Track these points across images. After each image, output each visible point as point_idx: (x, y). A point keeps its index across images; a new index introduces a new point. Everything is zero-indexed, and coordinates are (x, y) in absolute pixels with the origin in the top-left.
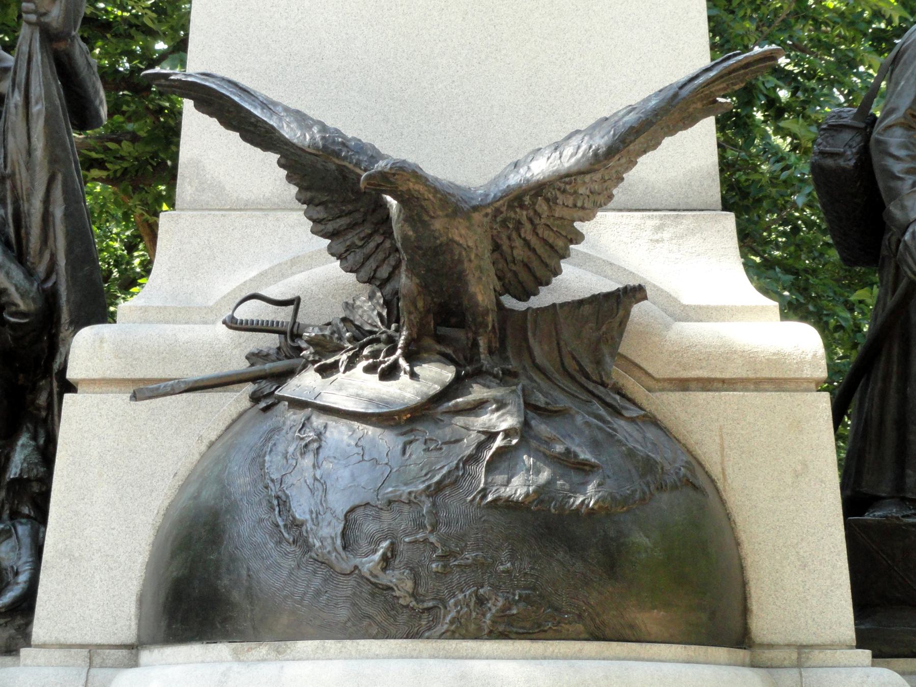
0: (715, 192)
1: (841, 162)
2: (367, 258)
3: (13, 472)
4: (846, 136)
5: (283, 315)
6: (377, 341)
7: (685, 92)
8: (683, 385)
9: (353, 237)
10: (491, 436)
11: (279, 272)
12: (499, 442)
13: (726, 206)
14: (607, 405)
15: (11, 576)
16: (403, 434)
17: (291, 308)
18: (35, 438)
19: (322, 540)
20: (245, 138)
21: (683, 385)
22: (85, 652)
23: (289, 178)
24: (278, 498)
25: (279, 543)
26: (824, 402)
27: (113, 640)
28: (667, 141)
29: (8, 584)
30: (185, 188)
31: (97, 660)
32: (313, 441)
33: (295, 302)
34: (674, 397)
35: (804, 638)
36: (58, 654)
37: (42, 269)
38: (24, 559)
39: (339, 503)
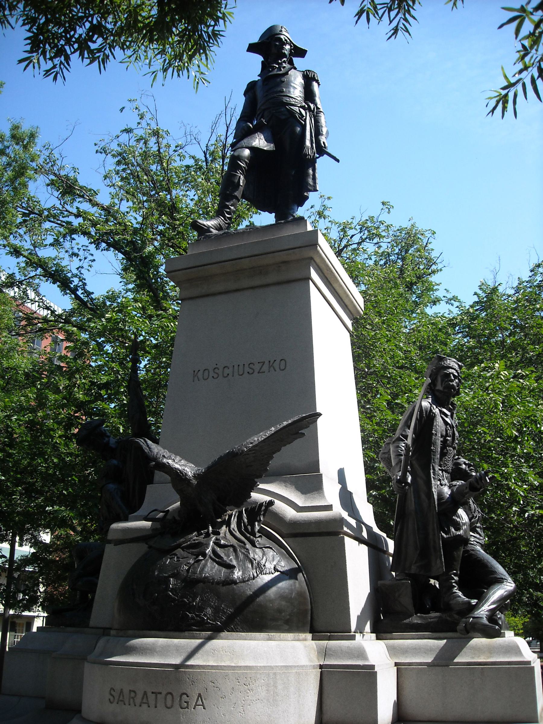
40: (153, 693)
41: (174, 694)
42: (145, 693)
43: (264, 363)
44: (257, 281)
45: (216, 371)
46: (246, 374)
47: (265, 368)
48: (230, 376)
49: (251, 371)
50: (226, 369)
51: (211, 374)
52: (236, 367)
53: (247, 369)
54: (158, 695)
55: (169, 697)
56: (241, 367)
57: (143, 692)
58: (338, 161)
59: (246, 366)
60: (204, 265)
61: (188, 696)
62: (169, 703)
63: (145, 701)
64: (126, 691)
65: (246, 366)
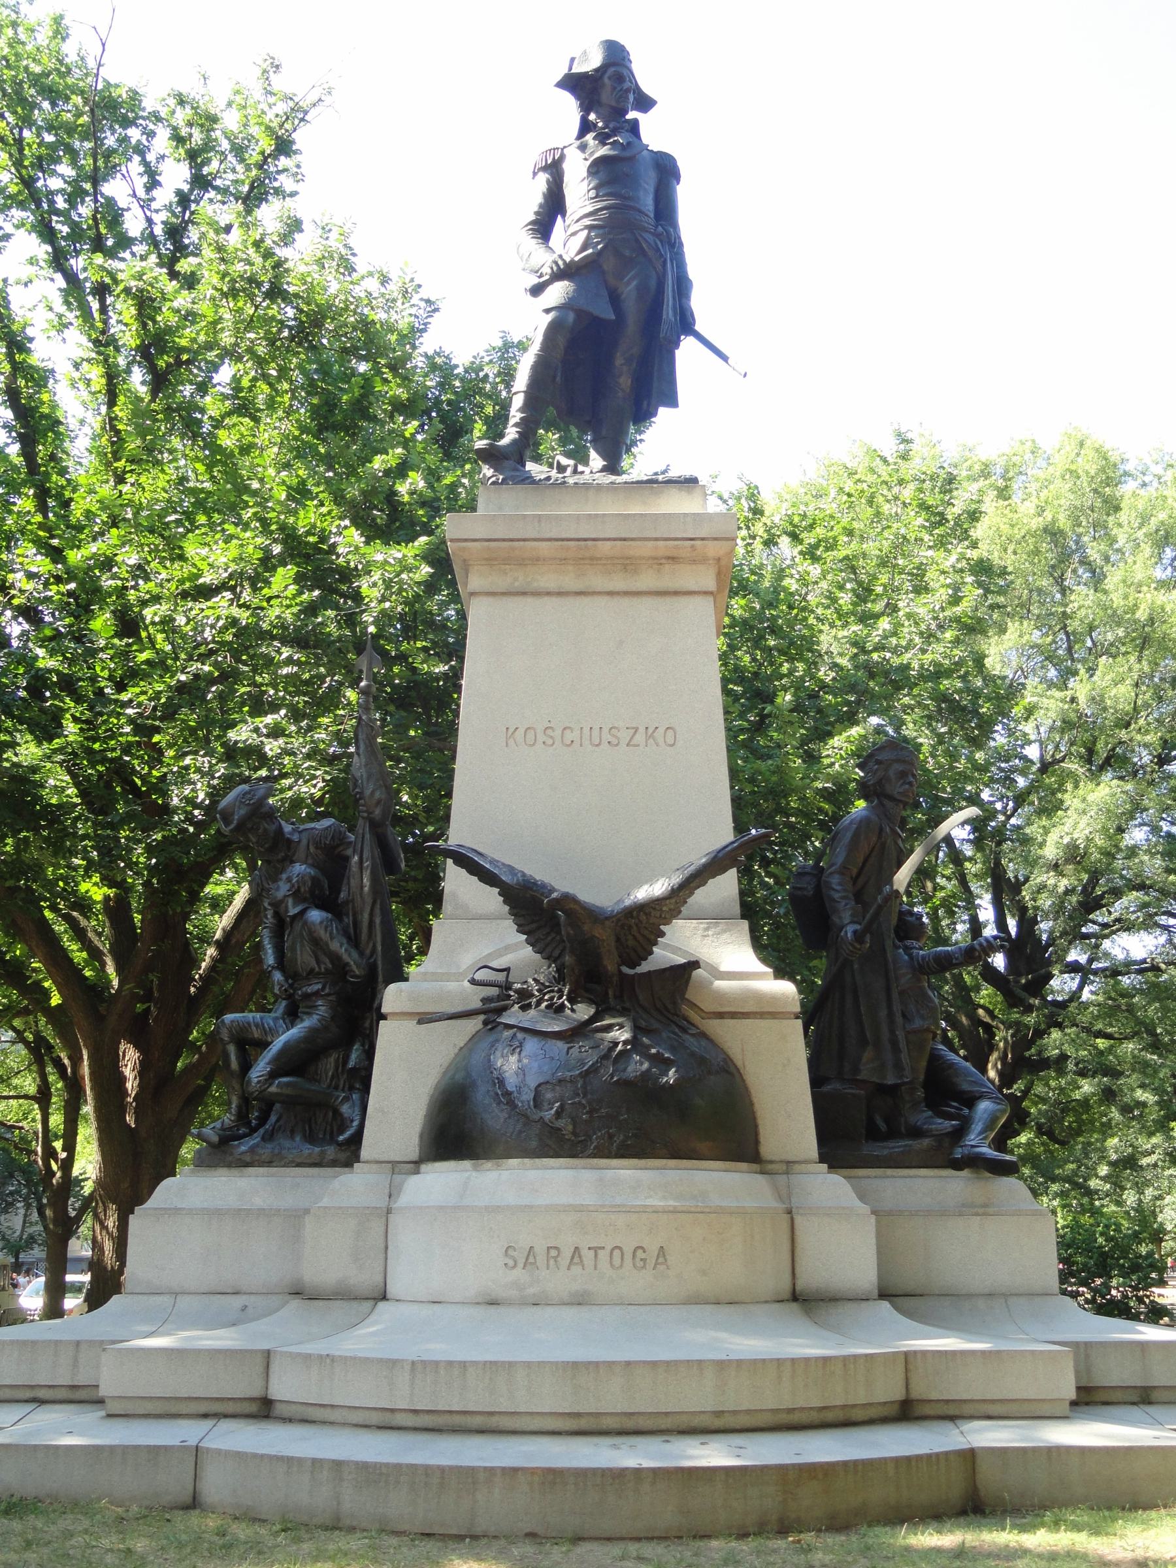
0: (737, 909)
2: (547, 945)
3: (351, 1064)
4: (808, 878)
5: (501, 977)
6: (552, 991)
7: (720, 855)
8: (721, 1015)
10: (616, 1044)
11: (499, 954)
12: (620, 1047)
13: (743, 917)
14: (677, 1025)
18: (363, 1045)
19: (522, 1102)
20: (481, 880)
21: (721, 1015)
23: (505, 902)
26: (799, 1024)
28: (710, 881)
30: (447, 906)
31: (397, 1170)
33: (507, 970)
34: (716, 1022)
35: (790, 1158)
36: (375, 1166)
37: (368, 952)
39: (532, 1082)
42: (577, 1248)
43: (636, 729)
44: (619, 583)
45: (549, 732)
46: (605, 745)
47: (640, 738)
48: (576, 745)
49: (615, 741)
50: (568, 732)
51: (541, 738)
52: (586, 731)
53: (606, 737)
54: (599, 1252)
55: (617, 1253)
56: (596, 732)
60: (524, 540)
63: (576, 1260)
64: (540, 1250)
65: (605, 730)
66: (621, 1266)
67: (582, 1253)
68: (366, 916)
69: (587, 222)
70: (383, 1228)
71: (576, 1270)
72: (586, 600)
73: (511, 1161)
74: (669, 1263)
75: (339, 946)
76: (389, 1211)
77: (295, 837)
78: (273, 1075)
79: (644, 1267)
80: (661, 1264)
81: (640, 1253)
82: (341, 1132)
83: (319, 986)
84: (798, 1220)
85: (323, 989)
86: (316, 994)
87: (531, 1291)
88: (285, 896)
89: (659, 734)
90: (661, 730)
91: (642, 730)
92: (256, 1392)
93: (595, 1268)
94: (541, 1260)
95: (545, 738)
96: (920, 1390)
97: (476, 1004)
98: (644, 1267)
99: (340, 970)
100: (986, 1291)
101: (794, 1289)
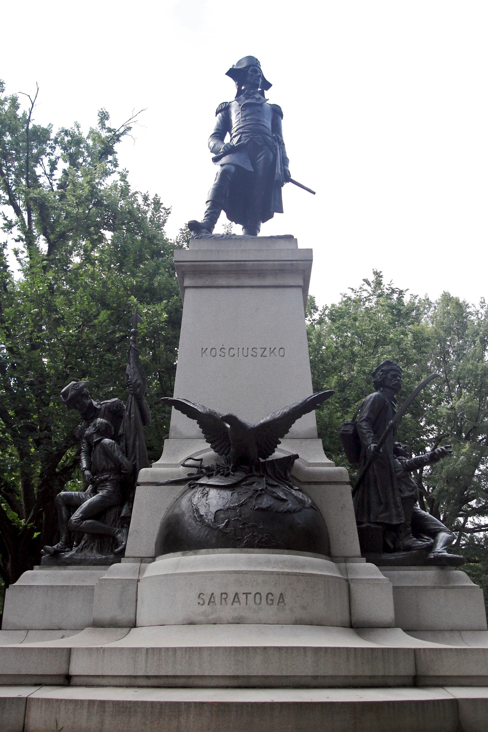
0: (316, 434)
1: (349, 433)
2: (221, 448)
3: (122, 515)
4: (349, 426)
6: (224, 468)
7: (308, 400)
9: (216, 443)
10: (257, 491)
11: (197, 454)
12: (259, 493)
13: (320, 436)
14: (289, 486)
15: (120, 543)
16: (232, 491)
17: (200, 462)
19: (208, 520)
20: (188, 416)
22: (140, 559)
23: (200, 427)
24: (196, 509)
25: (196, 522)
26: (349, 488)
27: (148, 556)
28: (303, 416)
29: (120, 545)
30: (172, 434)
31: (143, 561)
32: (206, 494)
33: (201, 460)
35: (346, 554)
36: (132, 559)
37: (132, 458)
38: (124, 538)
39: (213, 510)
40: (243, 594)
41: (262, 594)
42: (236, 594)
43: (266, 348)
45: (222, 350)
47: (267, 353)
49: (254, 354)
50: (231, 350)
51: (219, 353)
52: (241, 350)
54: (248, 595)
55: (258, 596)
56: (245, 350)
57: (234, 594)
58: (314, 193)
59: (250, 350)
61: (272, 596)
62: (258, 601)
63: (236, 600)
65: (250, 350)
66: (260, 603)
67: (239, 596)
68: (131, 440)
69: (240, 131)
70: (135, 590)
71: (236, 605)
72: (240, 290)
73: (202, 550)
74: (286, 602)
75: (119, 454)
76: (138, 581)
77: (99, 407)
78: (82, 519)
79: (272, 604)
80: (282, 602)
81: (270, 596)
82: (117, 547)
83: (108, 476)
84: (352, 585)
85: (109, 477)
86: (106, 480)
87: (212, 617)
88: (93, 433)
89: (276, 351)
90: (277, 349)
91: (268, 349)
92: (62, 671)
93: (247, 604)
94: (217, 600)
95: (221, 353)
96: (422, 671)
97: (185, 476)
98: (272, 604)
99: (118, 468)
100: (449, 629)
101: (351, 622)
